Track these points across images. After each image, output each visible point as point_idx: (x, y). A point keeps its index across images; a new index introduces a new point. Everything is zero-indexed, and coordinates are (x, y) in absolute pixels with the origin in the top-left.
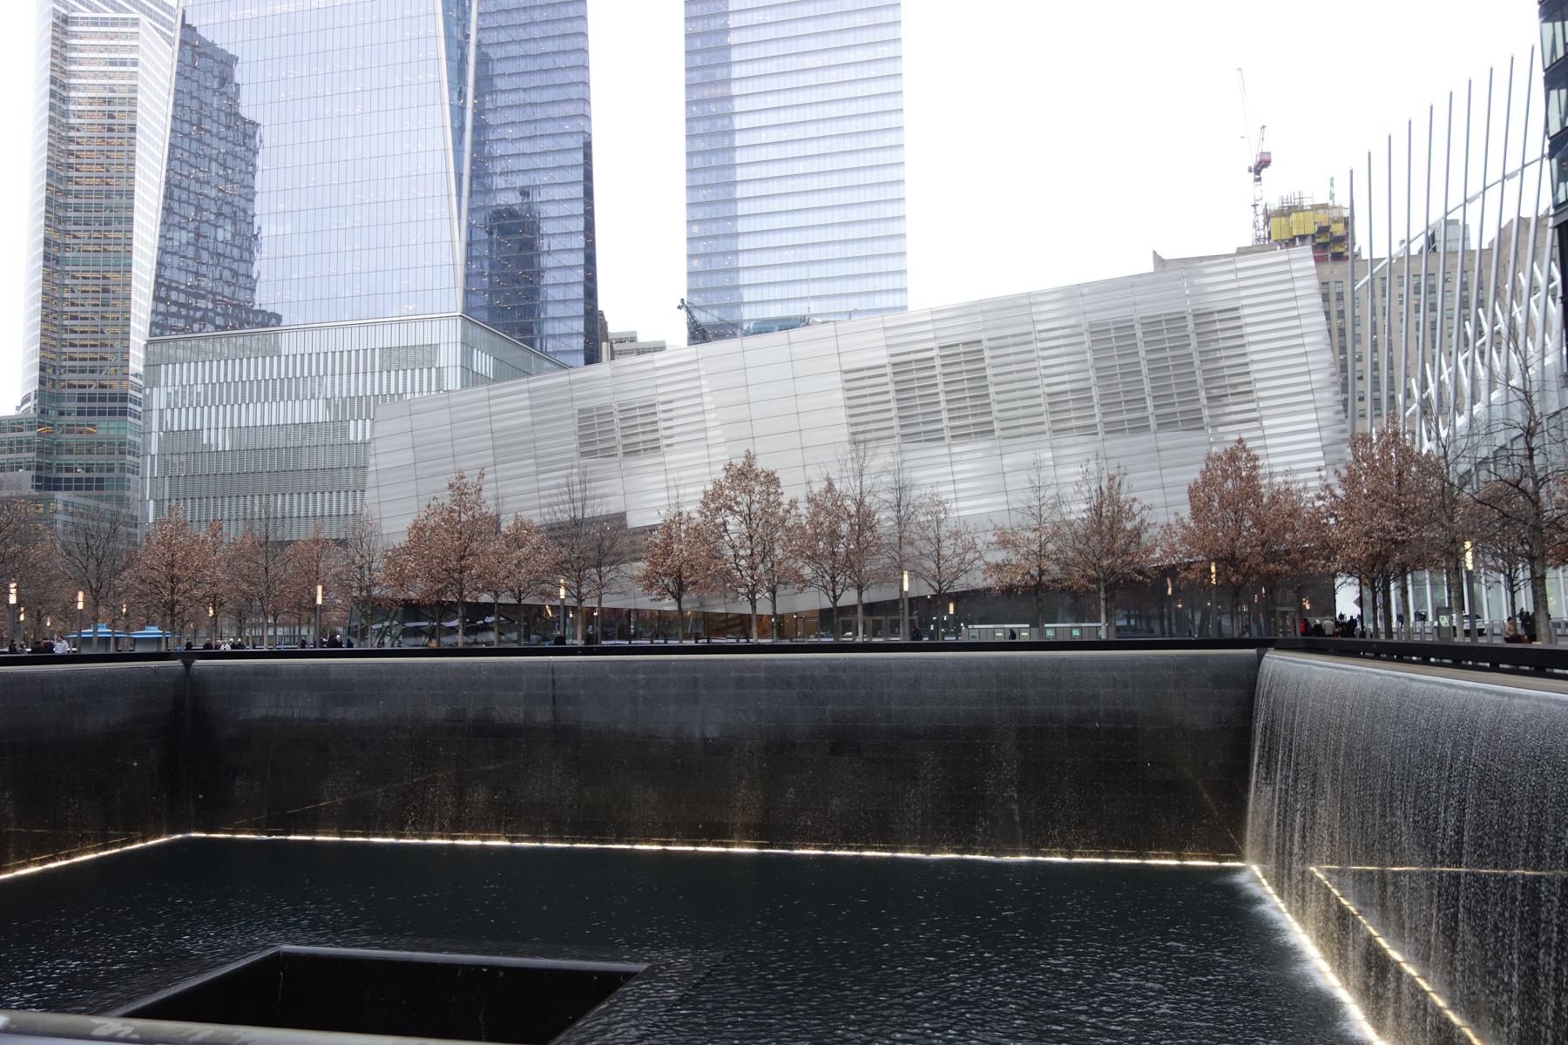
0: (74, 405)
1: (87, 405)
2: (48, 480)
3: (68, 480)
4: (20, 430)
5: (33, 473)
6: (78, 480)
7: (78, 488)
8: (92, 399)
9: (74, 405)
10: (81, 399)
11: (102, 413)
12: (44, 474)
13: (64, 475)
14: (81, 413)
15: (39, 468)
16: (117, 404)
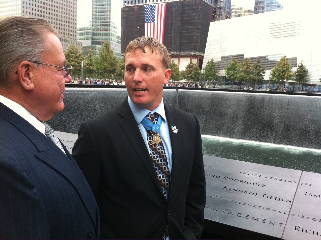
0: (99, 24)
1: (102, 24)
2: (94, 42)
3: (98, 42)
4: (88, 30)
5: (91, 40)
6: (100, 42)
7: (100, 44)
8: (103, 22)
9: (99, 24)
10: (100, 22)
11: (105, 26)
12: (93, 41)
13: (97, 41)
14: (100, 26)
15: (92, 39)
16: (108, 24)
